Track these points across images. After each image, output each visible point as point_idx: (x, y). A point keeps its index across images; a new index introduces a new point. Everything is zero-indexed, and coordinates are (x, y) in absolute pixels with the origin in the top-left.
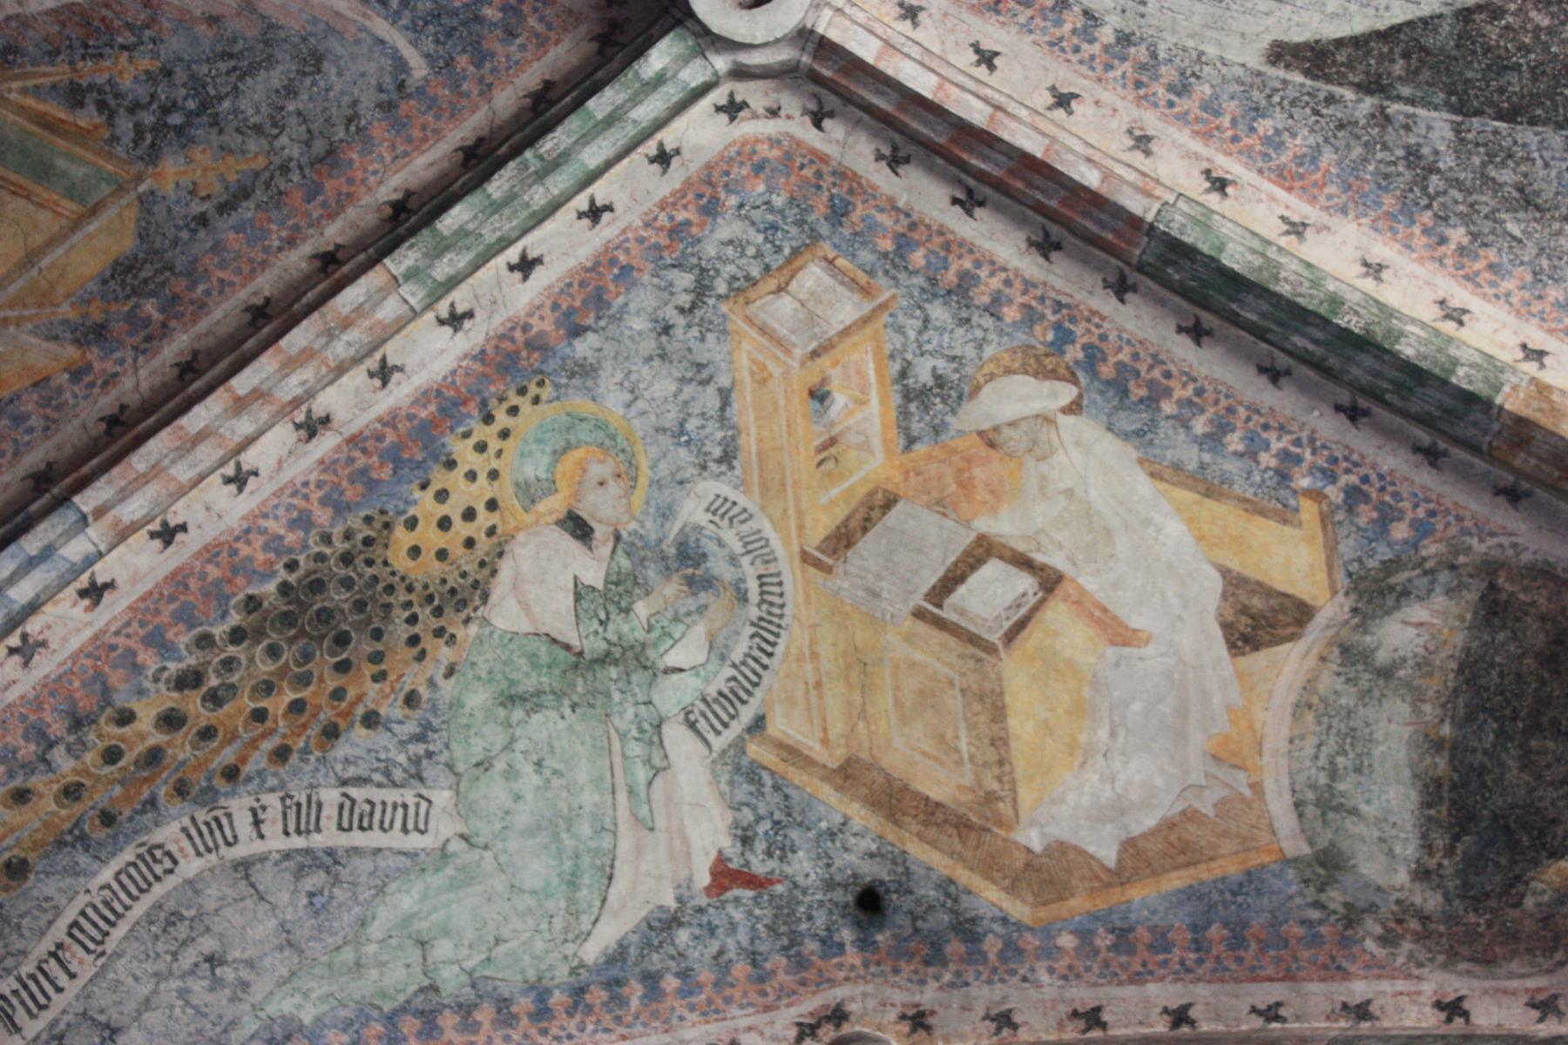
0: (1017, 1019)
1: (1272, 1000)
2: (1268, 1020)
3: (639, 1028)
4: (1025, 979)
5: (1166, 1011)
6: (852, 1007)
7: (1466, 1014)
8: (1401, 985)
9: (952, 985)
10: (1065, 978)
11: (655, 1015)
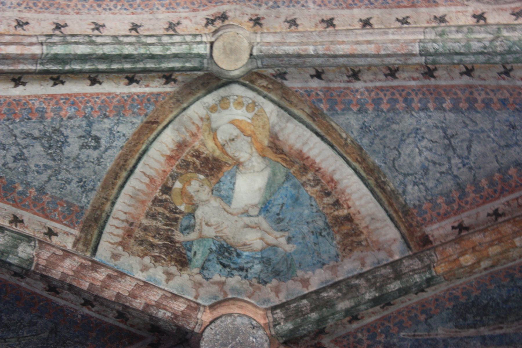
0: (298, 22)
1: (404, 16)
2: (403, 24)
3: (139, 11)
4: (303, 6)
5: (361, 20)
6: (229, 14)
7: (485, 19)
8: (459, 8)
9: (272, 7)
10: (320, 6)
11: (147, 6)
